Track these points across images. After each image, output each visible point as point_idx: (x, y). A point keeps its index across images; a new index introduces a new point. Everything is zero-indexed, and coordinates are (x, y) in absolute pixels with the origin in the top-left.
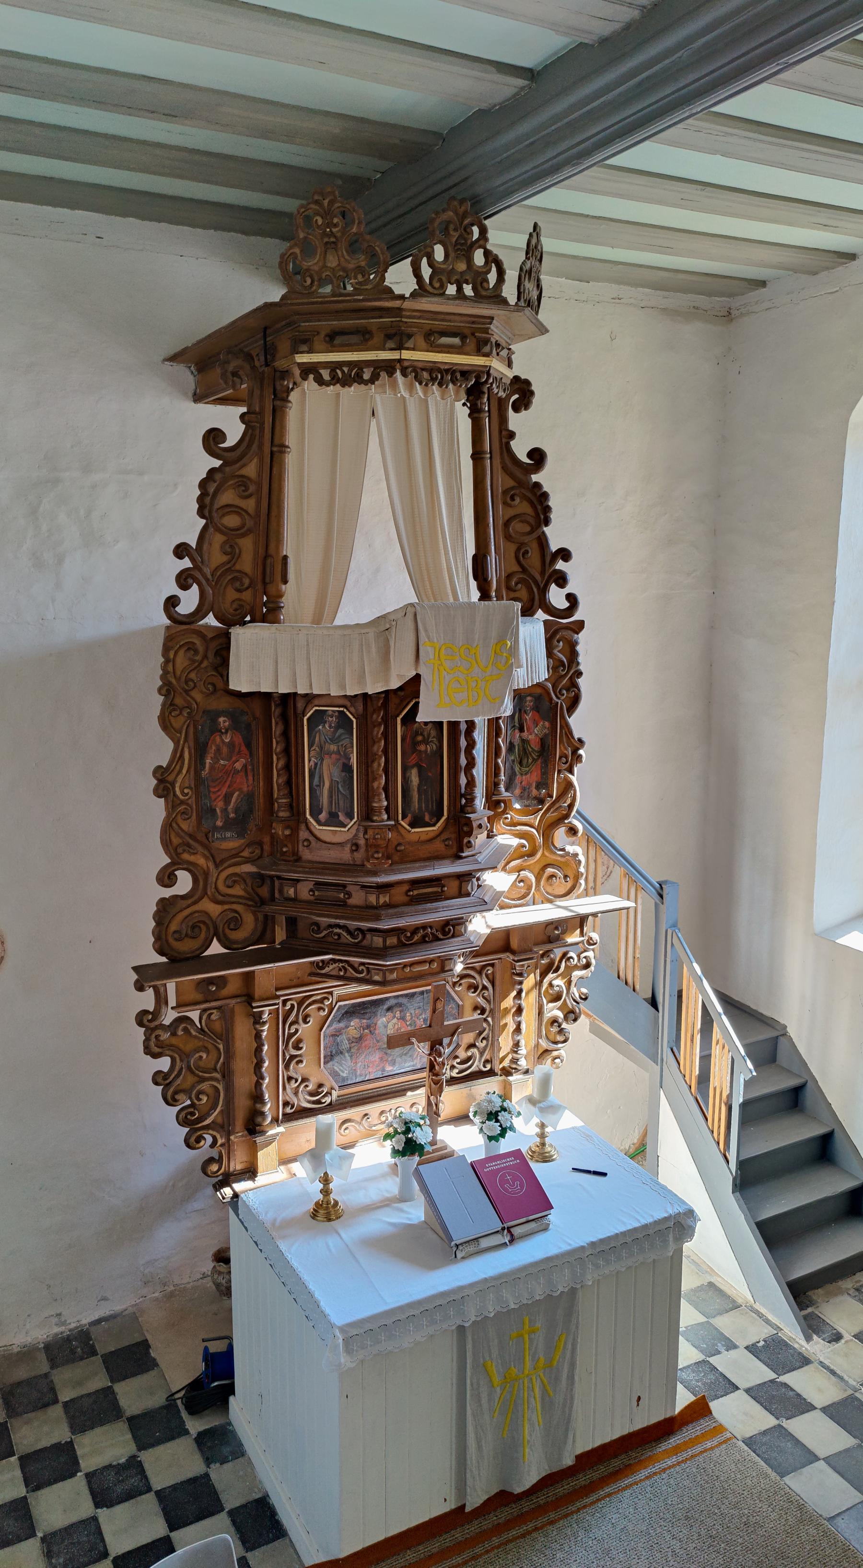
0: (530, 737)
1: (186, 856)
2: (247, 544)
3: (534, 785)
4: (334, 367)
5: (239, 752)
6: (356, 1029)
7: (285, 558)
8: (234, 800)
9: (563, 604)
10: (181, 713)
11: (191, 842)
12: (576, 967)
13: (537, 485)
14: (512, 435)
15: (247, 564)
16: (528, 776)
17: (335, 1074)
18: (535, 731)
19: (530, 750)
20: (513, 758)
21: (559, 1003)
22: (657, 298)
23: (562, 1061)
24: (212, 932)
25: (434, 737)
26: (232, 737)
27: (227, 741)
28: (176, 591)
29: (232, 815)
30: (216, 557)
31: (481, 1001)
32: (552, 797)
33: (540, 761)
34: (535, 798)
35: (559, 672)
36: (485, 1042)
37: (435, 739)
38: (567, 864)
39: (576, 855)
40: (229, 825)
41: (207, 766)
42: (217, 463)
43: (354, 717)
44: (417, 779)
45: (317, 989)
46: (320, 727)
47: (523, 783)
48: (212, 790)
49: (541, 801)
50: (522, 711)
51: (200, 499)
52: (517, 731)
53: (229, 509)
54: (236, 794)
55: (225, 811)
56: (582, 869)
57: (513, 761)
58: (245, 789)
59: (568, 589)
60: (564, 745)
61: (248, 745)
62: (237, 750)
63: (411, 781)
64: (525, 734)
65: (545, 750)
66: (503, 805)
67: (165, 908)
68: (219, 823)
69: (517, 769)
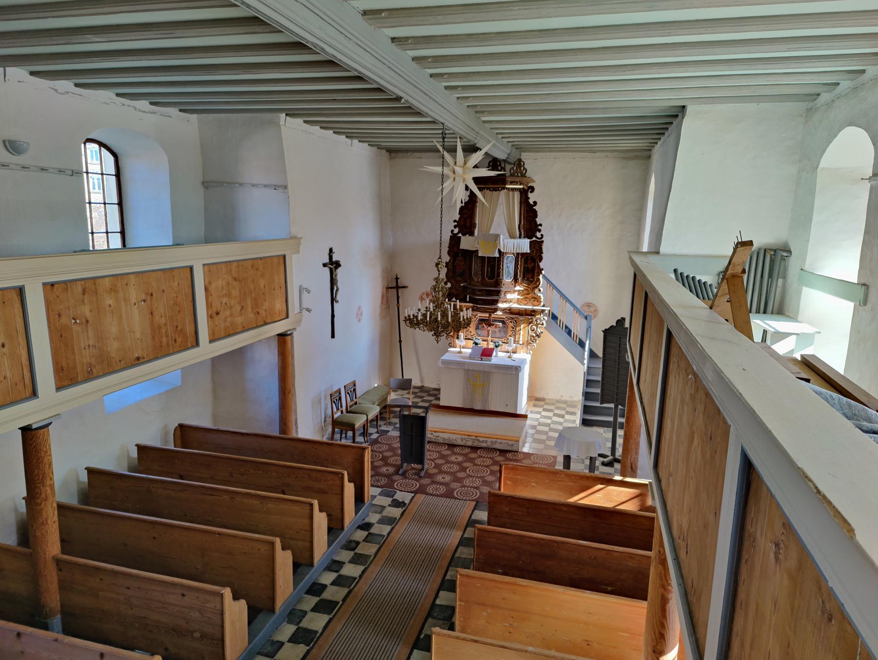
12: (539, 324)
13: (535, 209)
14: (529, 198)
15: (468, 224)
17: (477, 333)
39: (540, 296)
49: (532, 282)
56: (542, 300)
59: (541, 233)
64: (528, 266)
65: (533, 268)
68: (457, 274)
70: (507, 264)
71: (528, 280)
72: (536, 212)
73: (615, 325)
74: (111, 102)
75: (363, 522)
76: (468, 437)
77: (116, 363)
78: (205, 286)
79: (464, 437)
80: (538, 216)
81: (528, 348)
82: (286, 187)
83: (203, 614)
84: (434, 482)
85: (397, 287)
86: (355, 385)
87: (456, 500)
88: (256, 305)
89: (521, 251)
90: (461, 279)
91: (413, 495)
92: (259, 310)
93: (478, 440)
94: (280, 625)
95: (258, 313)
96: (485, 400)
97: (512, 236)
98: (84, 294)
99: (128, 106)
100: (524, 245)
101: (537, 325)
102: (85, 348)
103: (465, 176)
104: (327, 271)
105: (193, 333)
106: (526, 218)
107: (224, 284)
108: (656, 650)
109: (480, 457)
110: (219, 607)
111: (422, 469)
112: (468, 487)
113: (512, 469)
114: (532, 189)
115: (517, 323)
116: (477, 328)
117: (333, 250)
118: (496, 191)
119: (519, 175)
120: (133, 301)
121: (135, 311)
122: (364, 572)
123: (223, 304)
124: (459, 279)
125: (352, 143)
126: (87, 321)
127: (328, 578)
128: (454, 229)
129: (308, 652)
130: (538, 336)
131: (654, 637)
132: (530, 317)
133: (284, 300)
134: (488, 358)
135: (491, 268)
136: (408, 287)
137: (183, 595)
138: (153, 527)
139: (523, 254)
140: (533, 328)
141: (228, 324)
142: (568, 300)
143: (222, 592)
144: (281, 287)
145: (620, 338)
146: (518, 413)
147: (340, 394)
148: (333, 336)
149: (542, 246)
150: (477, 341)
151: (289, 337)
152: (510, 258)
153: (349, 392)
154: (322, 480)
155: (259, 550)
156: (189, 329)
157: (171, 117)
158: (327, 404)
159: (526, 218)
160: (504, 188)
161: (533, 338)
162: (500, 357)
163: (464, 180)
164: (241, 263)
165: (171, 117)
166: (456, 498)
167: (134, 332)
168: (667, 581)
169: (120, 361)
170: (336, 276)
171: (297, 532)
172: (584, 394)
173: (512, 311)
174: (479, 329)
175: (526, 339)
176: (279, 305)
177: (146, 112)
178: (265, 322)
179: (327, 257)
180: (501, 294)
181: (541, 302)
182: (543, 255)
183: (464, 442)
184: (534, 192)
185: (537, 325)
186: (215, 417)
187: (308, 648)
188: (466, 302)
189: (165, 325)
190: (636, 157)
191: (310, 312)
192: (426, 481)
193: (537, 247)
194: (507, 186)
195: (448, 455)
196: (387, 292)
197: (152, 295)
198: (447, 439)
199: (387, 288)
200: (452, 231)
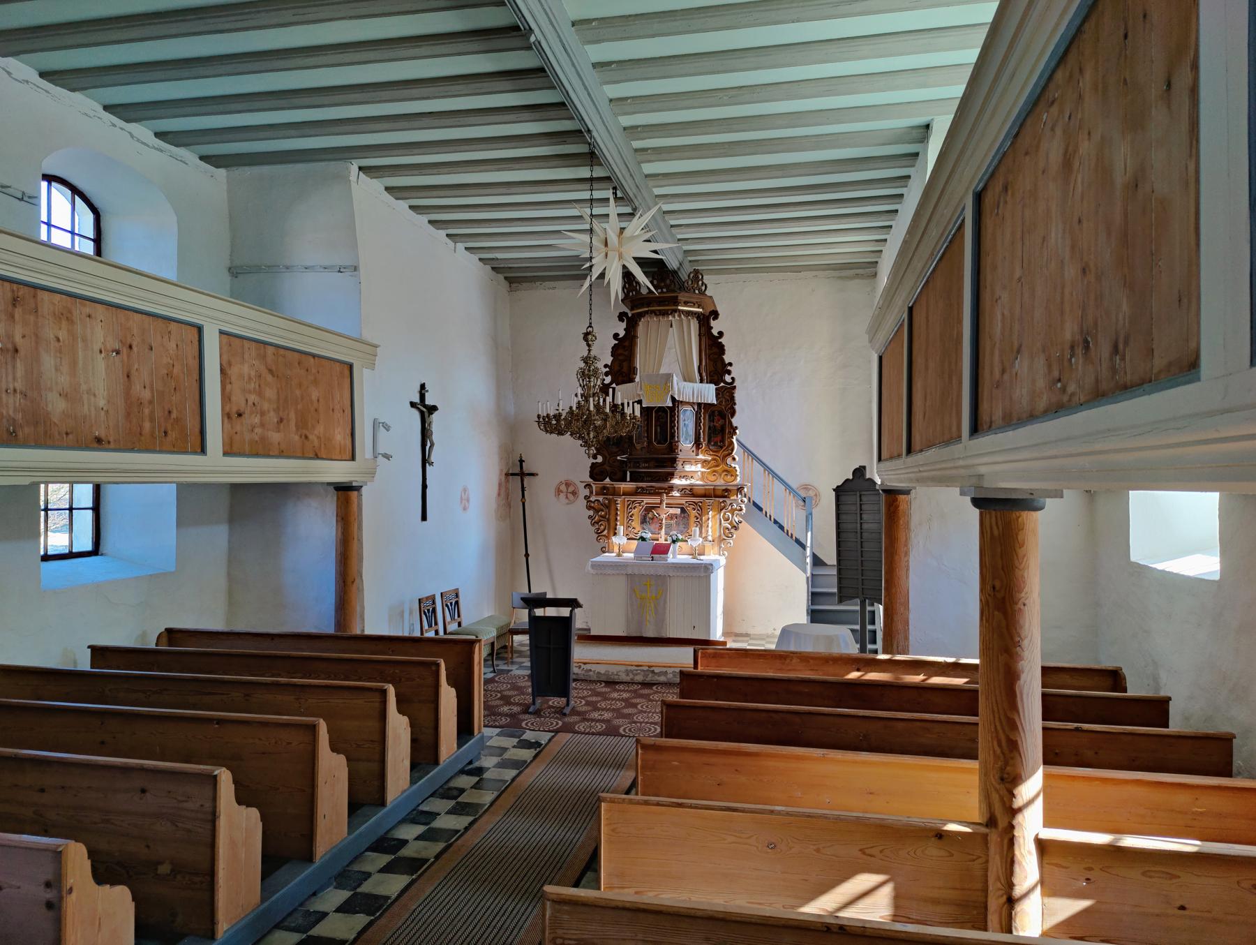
2: (625, 364)
4: (659, 310)
9: (730, 381)
13: (721, 342)
14: (712, 328)
21: (729, 522)
22: (837, 273)
31: (697, 515)
45: (638, 498)
49: (722, 447)
56: (738, 473)
67: (593, 466)
68: (611, 443)
70: (684, 420)
71: (715, 444)
72: (723, 346)
73: (851, 477)
74: (94, 116)
75: (470, 767)
76: (636, 668)
77: (59, 433)
78: (221, 365)
79: (629, 668)
81: (720, 547)
82: (356, 269)
83: (180, 825)
84: (585, 720)
85: (522, 475)
86: (457, 596)
87: (624, 738)
88: (302, 424)
89: (704, 400)
90: (617, 450)
91: (553, 734)
92: (308, 434)
93: (653, 672)
94: (323, 888)
95: (306, 437)
96: (661, 621)
97: (687, 378)
98: (14, 305)
99: (122, 129)
100: (708, 393)
101: (732, 511)
102: (7, 391)
103: (622, 250)
104: (416, 415)
105: (197, 430)
106: (709, 357)
107: (253, 373)
108: (1006, 776)
109: (656, 692)
110: (208, 805)
111: (568, 704)
112: (641, 723)
113: (713, 657)
114: (715, 314)
115: (701, 511)
116: (644, 521)
117: (426, 386)
118: (663, 315)
119: (697, 292)
120: (97, 347)
121: (100, 364)
122: (472, 824)
123: (250, 403)
124: (614, 449)
125: (455, 248)
126: (16, 351)
127: (409, 832)
129: (370, 924)
130: (736, 528)
131: (998, 751)
132: (721, 500)
133: (348, 431)
135: (660, 426)
136: (537, 475)
137: (143, 791)
138: (102, 724)
139: (706, 405)
140: (726, 516)
141: (257, 438)
142: (775, 476)
143: (216, 773)
144: (344, 411)
145: (860, 496)
146: (712, 638)
147: (434, 603)
148: (424, 518)
149: (733, 393)
150: (644, 535)
151: (355, 493)
152: (688, 413)
153: (449, 604)
154: (403, 679)
155: (289, 743)
156: (191, 423)
157: (187, 164)
158: (413, 624)
159: (709, 356)
160: (675, 311)
162: (677, 555)
163: (621, 257)
164: (282, 352)
165: (187, 164)
166: (622, 736)
167: (95, 395)
168: (1012, 638)
169: (67, 434)
170: (429, 425)
171: (358, 746)
172: (810, 611)
173: (695, 492)
174: (646, 522)
175: (718, 534)
176: (340, 437)
177: (148, 146)
178: (316, 455)
179: (418, 396)
180: (677, 465)
181: (737, 475)
182: (736, 407)
183: (631, 676)
184: (719, 319)
185: (732, 511)
186: (232, 602)
187: (372, 918)
188: (625, 480)
189: (151, 402)
190: (857, 276)
191: (389, 460)
192: (575, 718)
193: (727, 394)
194: (679, 308)
195: (606, 693)
196: (507, 481)
197: (130, 347)
198: (604, 674)
199: (507, 475)
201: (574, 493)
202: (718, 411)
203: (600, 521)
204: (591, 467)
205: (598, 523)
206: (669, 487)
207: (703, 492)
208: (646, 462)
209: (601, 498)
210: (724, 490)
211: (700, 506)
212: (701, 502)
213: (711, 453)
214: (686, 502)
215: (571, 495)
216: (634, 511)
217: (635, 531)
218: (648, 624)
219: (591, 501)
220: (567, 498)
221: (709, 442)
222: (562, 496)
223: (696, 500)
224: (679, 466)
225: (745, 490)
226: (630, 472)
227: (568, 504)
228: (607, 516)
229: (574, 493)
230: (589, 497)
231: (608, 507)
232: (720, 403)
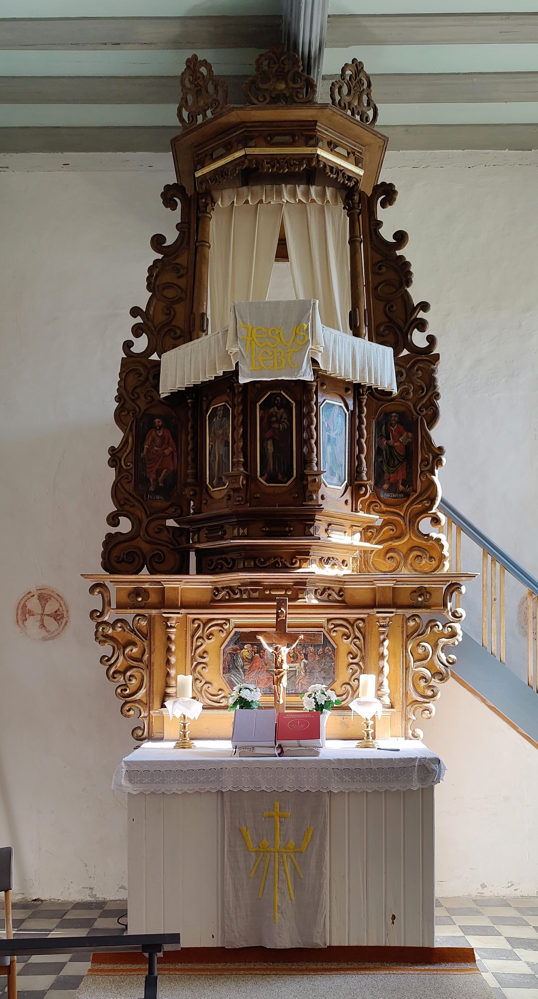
0: (396, 444)
1: (127, 507)
2: (180, 309)
3: (401, 481)
5: (168, 443)
6: (248, 652)
7: (203, 315)
8: (162, 475)
10: (128, 414)
11: (130, 498)
16: (395, 474)
18: (400, 439)
19: (396, 454)
20: (381, 459)
23: (430, 713)
24: (141, 561)
25: (285, 419)
26: (163, 433)
27: (160, 435)
28: (132, 338)
29: (161, 485)
30: (160, 318)
32: (416, 492)
33: (405, 463)
34: (402, 492)
35: (419, 395)
36: (356, 681)
37: (286, 420)
38: (432, 547)
40: (158, 490)
41: (145, 449)
42: (160, 256)
43: (231, 407)
44: (272, 448)
45: (217, 614)
46: (215, 420)
47: (391, 480)
48: (148, 466)
50: (389, 424)
51: (148, 279)
52: (384, 439)
53: (169, 286)
54: (164, 471)
55: (156, 480)
56: (446, 552)
57: (382, 462)
58: (172, 468)
60: (425, 450)
61: (175, 438)
62: (166, 442)
63: (268, 449)
64: (391, 441)
66: (364, 489)
68: (152, 489)
69: (385, 468)
71: (393, 489)
72: (408, 264)
80: (415, 278)
81: (407, 719)
90: (169, 503)
124: (159, 502)
128: (131, 337)
132: (409, 612)
134: (302, 742)
135: (273, 443)
149: (433, 371)
150: (246, 694)
159: (376, 288)
161: (422, 683)
200: (128, 345)
201: (58, 616)
202: (402, 415)
203: (130, 667)
204: (105, 544)
205: (124, 673)
206: (296, 584)
207: (367, 598)
208: (241, 524)
209: (129, 615)
210: (414, 591)
211: (359, 628)
212: (363, 620)
213: (384, 508)
214: (329, 620)
215: (53, 620)
216: (208, 644)
217: (211, 690)
218: (277, 915)
219: (105, 623)
220: (43, 626)
221: (378, 483)
222: (32, 623)
223: (352, 615)
224: (321, 533)
225: (463, 589)
226: (199, 552)
227: (45, 639)
228: (146, 656)
229: (58, 616)
230: (102, 614)
231: (147, 636)
232: (403, 393)
